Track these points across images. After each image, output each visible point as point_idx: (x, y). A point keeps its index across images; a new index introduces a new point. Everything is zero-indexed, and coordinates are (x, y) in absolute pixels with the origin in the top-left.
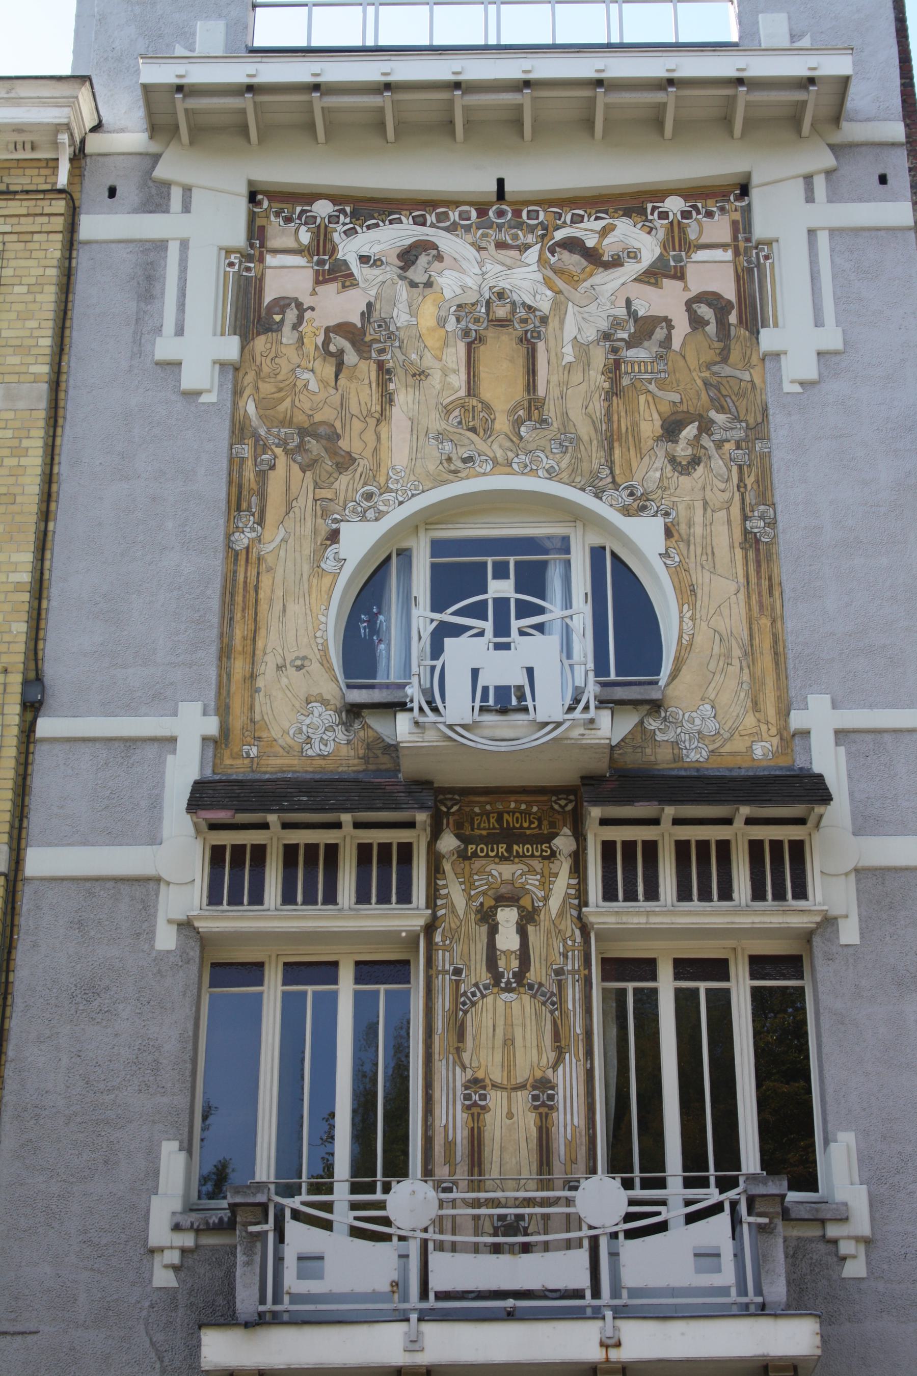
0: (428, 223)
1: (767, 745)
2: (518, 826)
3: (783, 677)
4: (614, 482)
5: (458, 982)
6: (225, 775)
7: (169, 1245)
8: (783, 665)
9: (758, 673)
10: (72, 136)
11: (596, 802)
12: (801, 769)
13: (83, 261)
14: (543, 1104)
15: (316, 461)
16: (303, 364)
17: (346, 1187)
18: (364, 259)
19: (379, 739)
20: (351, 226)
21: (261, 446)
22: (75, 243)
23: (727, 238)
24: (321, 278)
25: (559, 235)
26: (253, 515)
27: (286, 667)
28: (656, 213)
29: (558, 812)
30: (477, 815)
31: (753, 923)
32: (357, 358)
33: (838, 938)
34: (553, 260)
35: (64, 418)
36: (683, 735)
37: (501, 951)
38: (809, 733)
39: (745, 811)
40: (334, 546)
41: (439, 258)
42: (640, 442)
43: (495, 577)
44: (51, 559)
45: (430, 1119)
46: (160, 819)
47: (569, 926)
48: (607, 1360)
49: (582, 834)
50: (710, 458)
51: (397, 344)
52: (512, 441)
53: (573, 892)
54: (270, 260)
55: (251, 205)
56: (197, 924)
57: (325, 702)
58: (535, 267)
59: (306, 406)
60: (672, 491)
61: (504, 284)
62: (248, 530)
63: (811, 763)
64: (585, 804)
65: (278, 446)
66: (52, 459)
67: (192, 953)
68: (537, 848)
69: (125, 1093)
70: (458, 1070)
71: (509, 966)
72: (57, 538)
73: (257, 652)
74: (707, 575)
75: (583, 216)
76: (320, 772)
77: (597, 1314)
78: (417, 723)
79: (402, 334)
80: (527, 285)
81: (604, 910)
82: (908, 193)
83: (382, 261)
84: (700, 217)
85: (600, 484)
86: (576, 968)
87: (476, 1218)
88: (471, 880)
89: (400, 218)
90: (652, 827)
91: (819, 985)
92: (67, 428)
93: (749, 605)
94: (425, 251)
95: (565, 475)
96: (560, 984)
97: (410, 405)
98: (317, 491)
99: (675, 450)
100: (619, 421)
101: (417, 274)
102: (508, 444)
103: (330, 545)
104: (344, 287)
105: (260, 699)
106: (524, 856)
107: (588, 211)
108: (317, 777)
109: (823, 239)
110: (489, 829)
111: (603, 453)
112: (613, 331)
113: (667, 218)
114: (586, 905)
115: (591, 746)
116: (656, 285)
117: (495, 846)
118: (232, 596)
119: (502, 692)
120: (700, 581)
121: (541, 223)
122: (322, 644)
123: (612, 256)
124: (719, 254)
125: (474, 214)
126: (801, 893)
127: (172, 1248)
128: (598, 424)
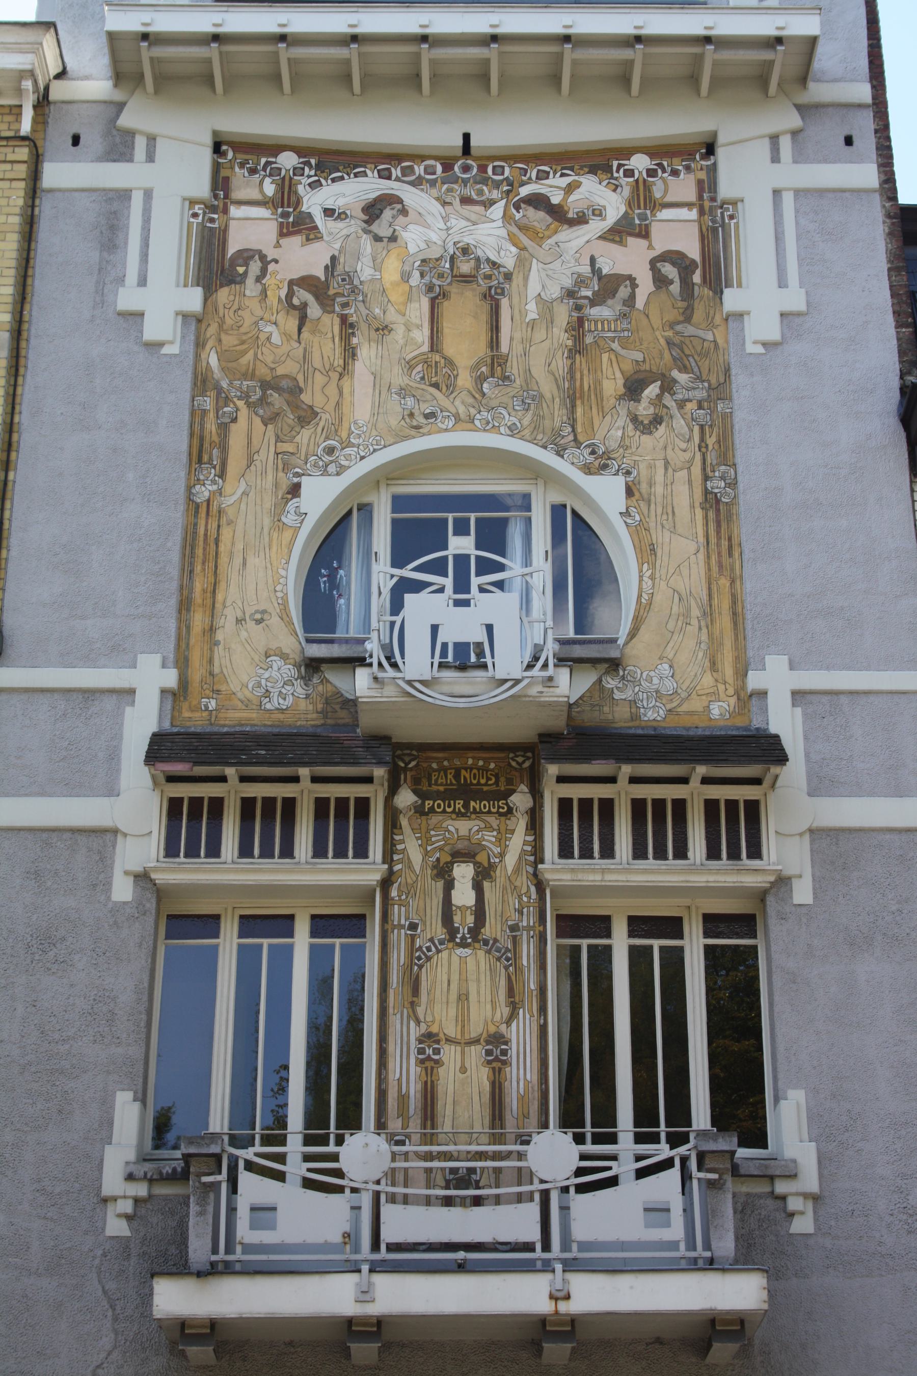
0: (394, 177)
1: (725, 705)
2: (475, 782)
3: (741, 637)
4: (575, 439)
5: (413, 937)
6: (183, 727)
7: (122, 1194)
8: (741, 626)
10: (35, 82)
11: (553, 759)
12: (757, 729)
13: (46, 209)
14: (497, 1059)
15: (278, 414)
16: (266, 316)
17: (300, 1138)
18: (328, 212)
19: (338, 694)
20: (316, 178)
21: (223, 399)
22: (38, 191)
23: (692, 196)
24: (285, 231)
25: (524, 191)
26: (214, 468)
28: (621, 171)
29: (516, 769)
30: (435, 771)
31: (708, 882)
32: (320, 312)
33: (791, 898)
34: (518, 216)
35: (26, 367)
36: (640, 693)
37: (458, 907)
38: (766, 693)
39: (702, 770)
40: (295, 500)
41: (404, 212)
42: (602, 400)
43: (456, 533)
44: (11, 509)
45: (384, 1072)
46: (118, 771)
47: (525, 883)
48: (557, 1312)
49: (539, 791)
50: (671, 417)
51: (361, 298)
52: (474, 397)
53: (529, 848)
54: (235, 211)
55: (215, 156)
56: (153, 876)
57: (284, 657)
58: (500, 223)
59: (269, 359)
60: (634, 450)
62: (209, 482)
63: (768, 724)
64: (543, 761)
65: (240, 398)
66: (13, 408)
67: (148, 905)
68: (494, 804)
69: (80, 1044)
70: (412, 1024)
71: (464, 921)
72: (18, 487)
73: (217, 605)
74: (667, 534)
75: (548, 173)
76: (279, 726)
77: (547, 1267)
79: (366, 288)
80: (491, 241)
81: (560, 867)
82: (873, 155)
83: (346, 214)
84: (665, 175)
86: (531, 924)
87: (428, 1171)
88: (428, 835)
89: (365, 172)
90: (608, 785)
91: (772, 945)
92: (28, 377)
93: (709, 564)
94: (390, 205)
95: (527, 433)
96: (515, 941)
97: (373, 360)
98: (279, 444)
99: (637, 409)
100: (582, 379)
101: (381, 227)
102: (471, 400)
103: (291, 499)
104: (308, 239)
105: (219, 652)
106: (481, 812)
107: (554, 167)
108: (276, 730)
109: (788, 199)
110: (446, 784)
111: (565, 411)
112: (576, 289)
113: (633, 176)
114: (542, 862)
115: (550, 704)
116: (621, 243)
117: (452, 802)
118: (193, 548)
119: (462, 648)
120: (660, 541)
121: (507, 179)
122: (282, 598)
123: (577, 213)
125: (439, 169)
126: (755, 852)
127: (125, 1197)
128: (561, 382)
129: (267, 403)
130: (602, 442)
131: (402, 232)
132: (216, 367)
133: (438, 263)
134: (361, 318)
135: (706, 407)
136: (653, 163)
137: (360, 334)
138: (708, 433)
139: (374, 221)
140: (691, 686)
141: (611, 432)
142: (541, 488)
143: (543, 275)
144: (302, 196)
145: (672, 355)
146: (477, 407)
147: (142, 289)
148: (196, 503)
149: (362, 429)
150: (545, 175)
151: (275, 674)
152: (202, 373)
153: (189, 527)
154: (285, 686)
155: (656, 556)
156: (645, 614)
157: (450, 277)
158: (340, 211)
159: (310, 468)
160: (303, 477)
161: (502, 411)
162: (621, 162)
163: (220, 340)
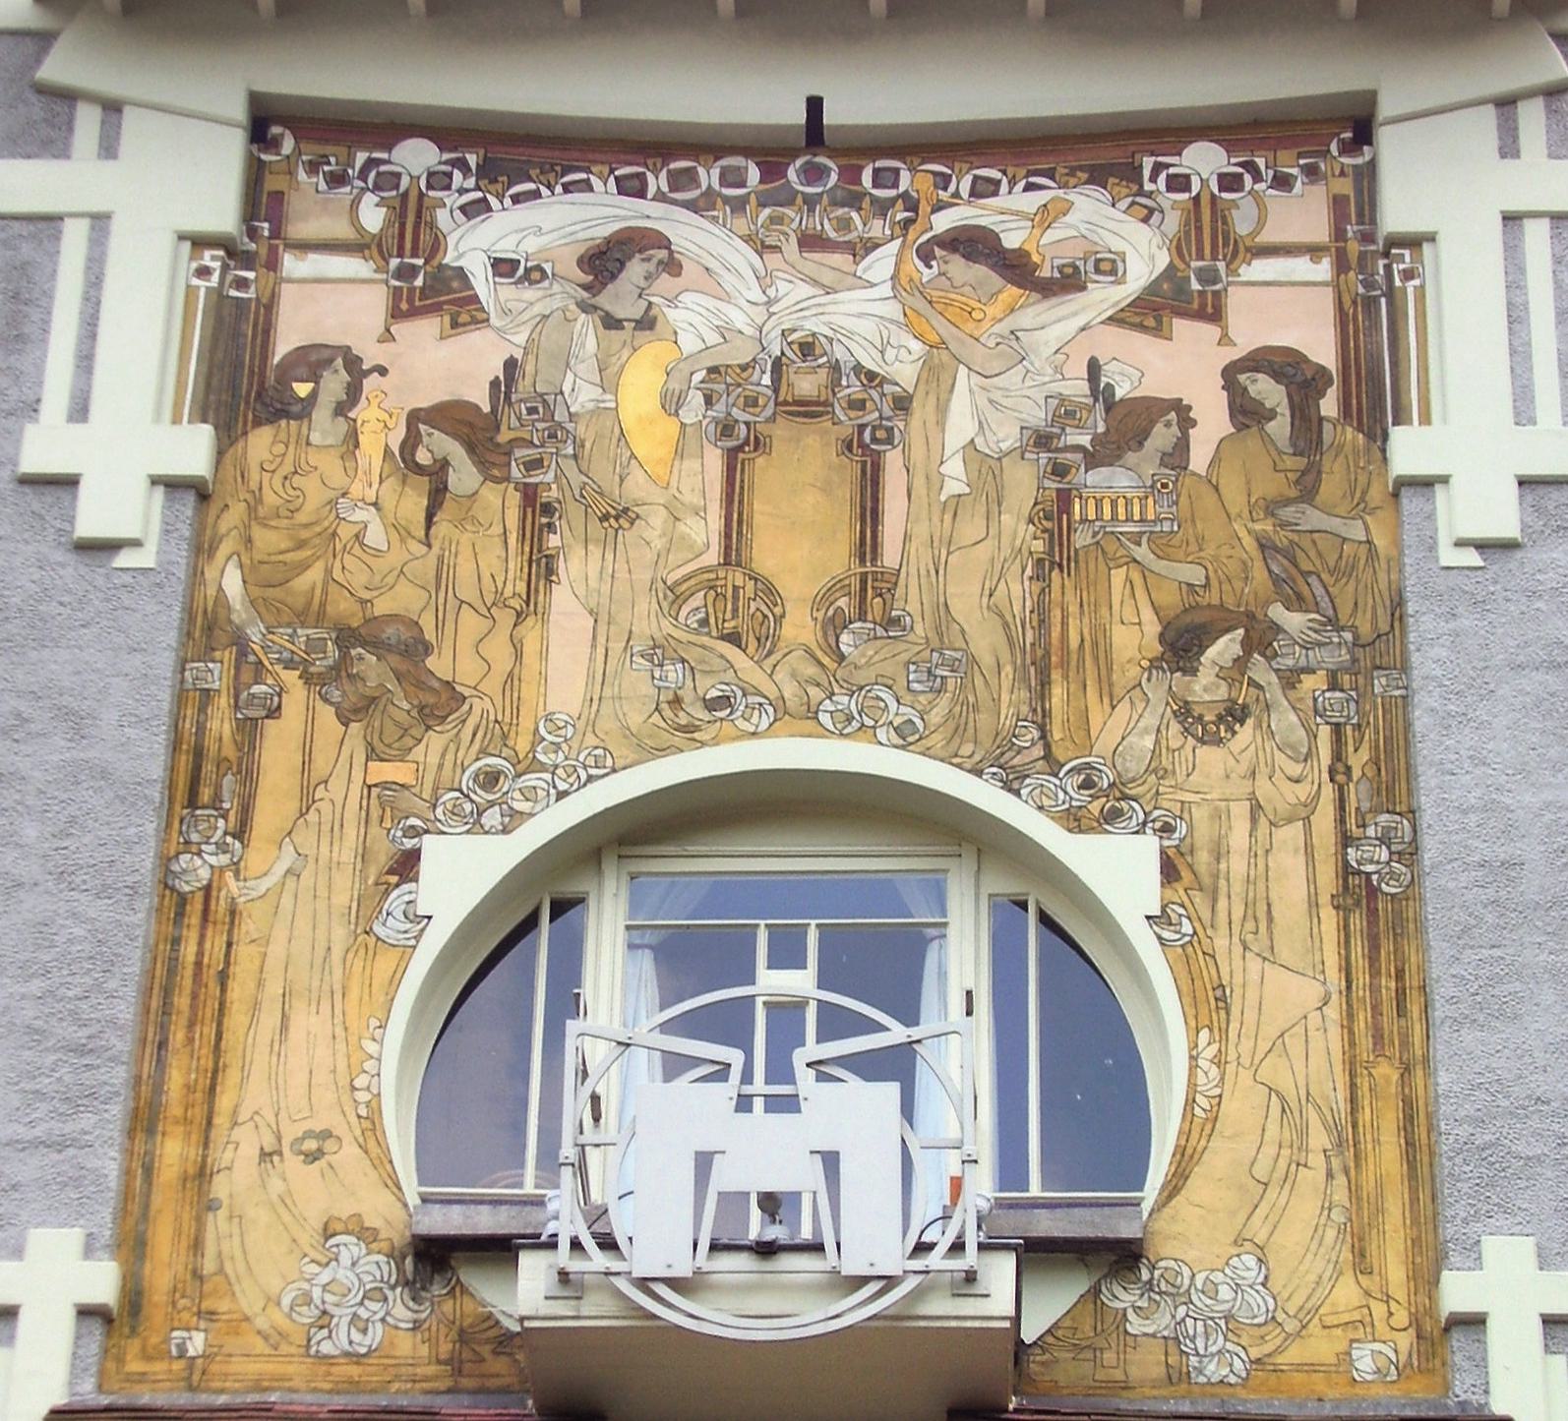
0: (651, 191)
3: (1424, 1196)
4: (1048, 756)
8: (1426, 1169)
9: (1368, 1184)
18: (503, 267)
20: (480, 194)
21: (247, 664)
23: (1319, 231)
25: (943, 222)
26: (225, 817)
27: (280, 1154)
28: (1162, 178)
36: (1189, 1322)
38: (1484, 1322)
40: (406, 887)
41: (672, 266)
42: (1110, 670)
51: (570, 451)
54: (292, 264)
55: (254, 148)
57: (366, 1235)
58: (886, 290)
59: (358, 578)
60: (1180, 777)
61: (812, 325)
62: (211, 848)
63: (1486, 1392)
65: (289, 665)
73: (217, 1121)
74: (1254, 965)
78: (564, 1276)
80: (867, 328)
83: (543, 271)
84: (1260, 186)
85: (1015, 761)
94: (640, 251)
95: (937, 740)
97: (593, 583)
99: (1188, 688)
100: (1064, 624)
101: (621, 299)
102: (812, 670)
103: (397, 885)
104: (455, 325)
105: (217, 1224)
107: (1010, 171)
109: (1537, 234)
111: (1024, 694)
113: (1187, 188)
116: (1159, 331)
118: (167, 992)
119: (771, 1204)
120: (1238, 980)
121: (905, 196)
122: (368, 1104)
123: (1060, 269)
124: (1301, 268)
125: (754, 174)
129: (349, 676)
130: (1109, 763)
131: (665, 310)
132: (239, 598)
133: (745, 375)
134: (568, 493)
135: (1347, 686)
136: (1233, 160)
137: (565, 527)
138: (1350, 741)
139: (604, 285)
140: (1309, 1305)
141: (1128, 739)
142: (969, 863)
143: (982, 402)
144: (445, 231)
145: (1270, 571)
146: (826, 685)
147: (79, 427)
148: (179, 893)
149: (562, 732)
150: (992, 188)
151: (344, 1275)
152: (205, 612)
153: (161, 947)
154: (366, 1302)
155: (1228, 1014)
156: (1203, 1142)
157: (772, 404)
158: (529, 264)
159: (442, 818)
160: (426, 837)
161: (880, 694)
162: (1160, 159)
163: (249, 540)
